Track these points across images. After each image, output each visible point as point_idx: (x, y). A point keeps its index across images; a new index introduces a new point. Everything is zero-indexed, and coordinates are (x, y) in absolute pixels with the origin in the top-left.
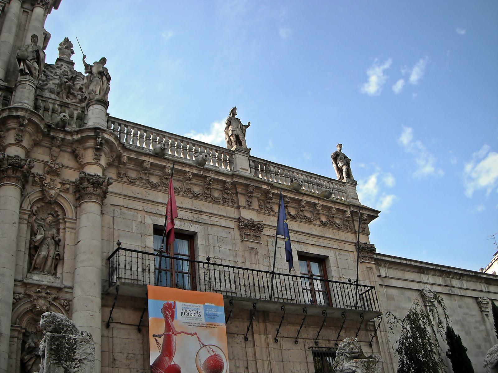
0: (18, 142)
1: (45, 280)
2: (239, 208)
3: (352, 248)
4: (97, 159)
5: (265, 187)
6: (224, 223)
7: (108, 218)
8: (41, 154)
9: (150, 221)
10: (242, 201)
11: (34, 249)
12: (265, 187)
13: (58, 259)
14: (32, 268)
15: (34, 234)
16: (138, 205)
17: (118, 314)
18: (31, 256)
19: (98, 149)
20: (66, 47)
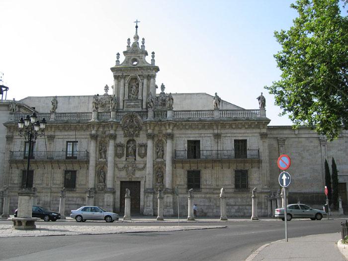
0: (150, 129)
1: (159, 160)
2: (214, 130)
3: (259, 135)
4: (169, 128)
5: (221, 122)
6: (208, 135)
7: (175, 141)
8: (157, 128)
9: (186, 139)
10: (215, 127)
11: (158, 153)
12: (221, 122)
13: (163, 154)
14: (158, 158)
15: (157, 149)
16: (183, 136)
17: (177, 165)
18: (157, 154)
19: (169, 125)
20: (163, 87)
